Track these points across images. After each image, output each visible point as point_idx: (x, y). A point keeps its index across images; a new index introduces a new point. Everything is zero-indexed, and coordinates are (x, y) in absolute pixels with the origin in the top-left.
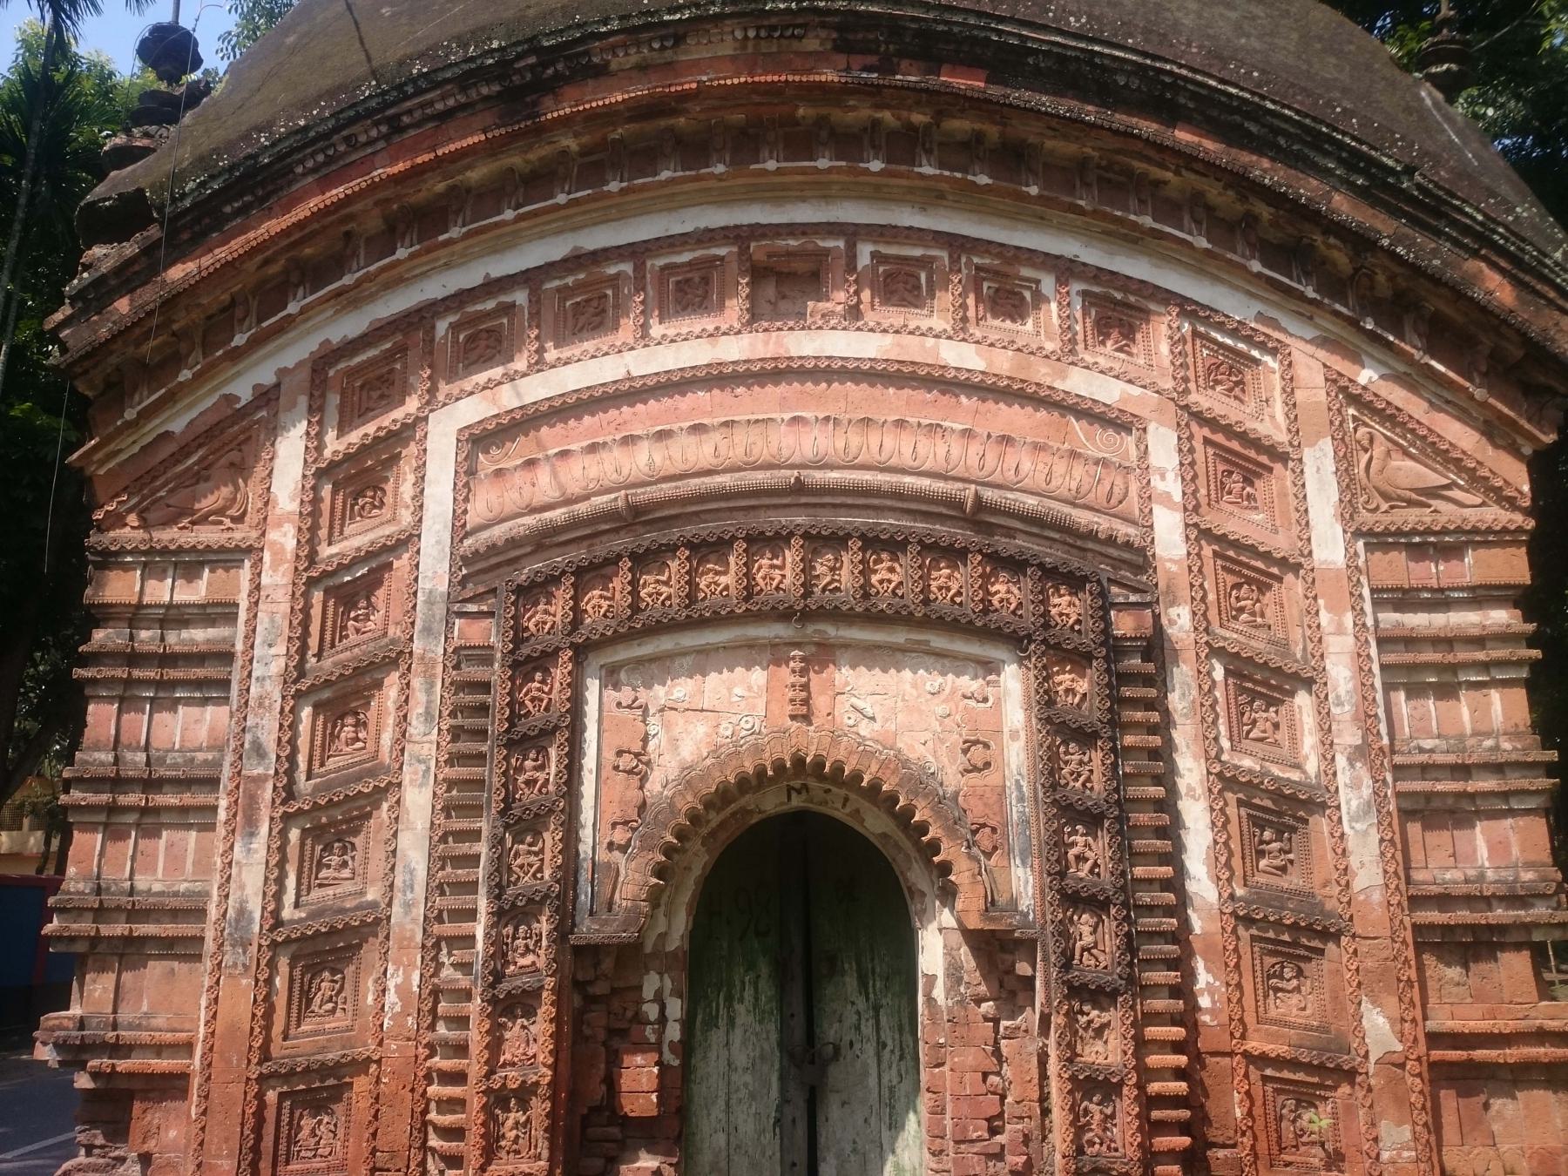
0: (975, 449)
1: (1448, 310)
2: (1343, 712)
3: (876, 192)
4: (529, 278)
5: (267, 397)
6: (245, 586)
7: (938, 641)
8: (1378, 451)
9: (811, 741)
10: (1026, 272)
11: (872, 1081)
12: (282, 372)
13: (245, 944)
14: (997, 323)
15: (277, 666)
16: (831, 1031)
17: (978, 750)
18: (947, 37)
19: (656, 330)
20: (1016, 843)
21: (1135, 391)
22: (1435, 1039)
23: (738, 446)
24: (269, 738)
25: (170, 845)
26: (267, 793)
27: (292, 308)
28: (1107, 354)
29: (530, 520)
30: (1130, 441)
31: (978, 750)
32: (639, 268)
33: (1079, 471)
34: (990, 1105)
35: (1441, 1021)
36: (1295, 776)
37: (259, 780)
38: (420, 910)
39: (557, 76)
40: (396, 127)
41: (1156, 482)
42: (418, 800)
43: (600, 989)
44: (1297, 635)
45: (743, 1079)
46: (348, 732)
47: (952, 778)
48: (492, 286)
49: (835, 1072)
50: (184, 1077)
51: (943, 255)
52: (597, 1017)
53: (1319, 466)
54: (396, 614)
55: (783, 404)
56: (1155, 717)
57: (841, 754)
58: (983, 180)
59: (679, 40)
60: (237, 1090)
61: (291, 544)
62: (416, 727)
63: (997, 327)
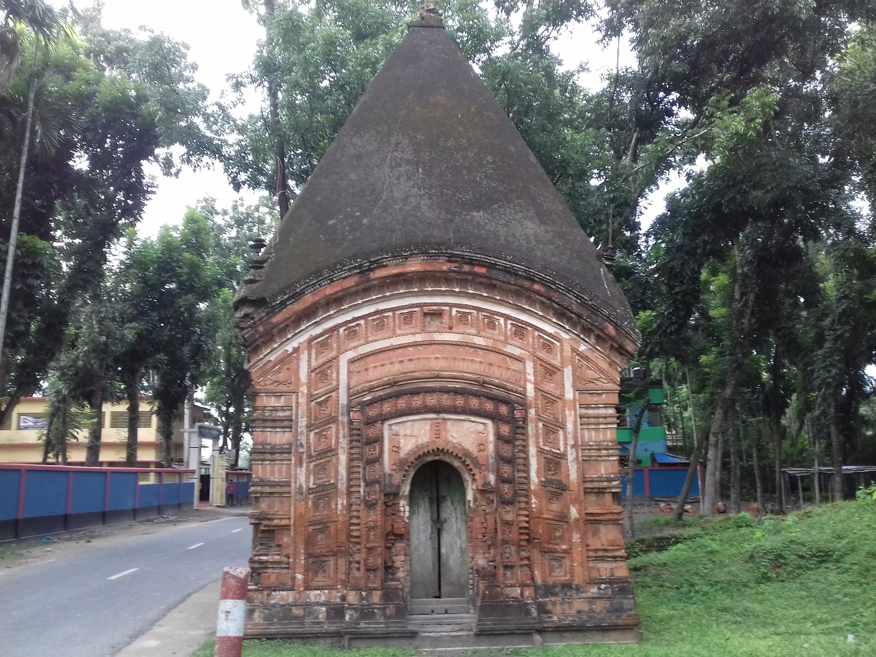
0: (483, 366)
1: (601, 334)
2: (570, 436)
3: (458, 295)
4: (364, 317)
5: (296, 350)
6: (294, 401)
7: (473, 419)
8: (584, 367)
9: (440, 444)
10: (496, 317)
11: (454, 527)
12: (300, 343)
13: (301, 494)
14: (488, 330)
15: (304, 423)
16: (443, 515)
17: (482, 446)
18: (476, 260)
19: (398, 332)
20: (491, 468)
21: (523, 352)
22: (587, 514)
23: (421, 365)
24: (304, 442)
25: (279, 470)
26: (305, 456)
27: (303, 327)
28: (517, 341)
29: (367, 385)
30: (521, 364)
31: (482, 446)
32: (394, 314)
33: (509, 372)
34: (484, 530)
35: (590, 510)
36: (558, 452)
37: (303, 453)
38: (345, 485)
39: (375, 268)
40: (332, 281)
41: (528, 377)
42: (343, 458)
43: (390, 504)
44: (560, 416)
45: (422, 527)
46: (323, 440)
47: (475, 453)
48: (355, 319)
49: (445, 525)
50: (289, 526)
51: (475, 312)
52: (389, 510)
53: (568, 372)
54: (333, 410)
55: (433, 353)
56: (524, 438)
57: (448, 447)
58: (485, 295)
59: (406, 258)
60: (303, 529)
61: (306, 391)
62: (341, 440)
63: (489, 332)
